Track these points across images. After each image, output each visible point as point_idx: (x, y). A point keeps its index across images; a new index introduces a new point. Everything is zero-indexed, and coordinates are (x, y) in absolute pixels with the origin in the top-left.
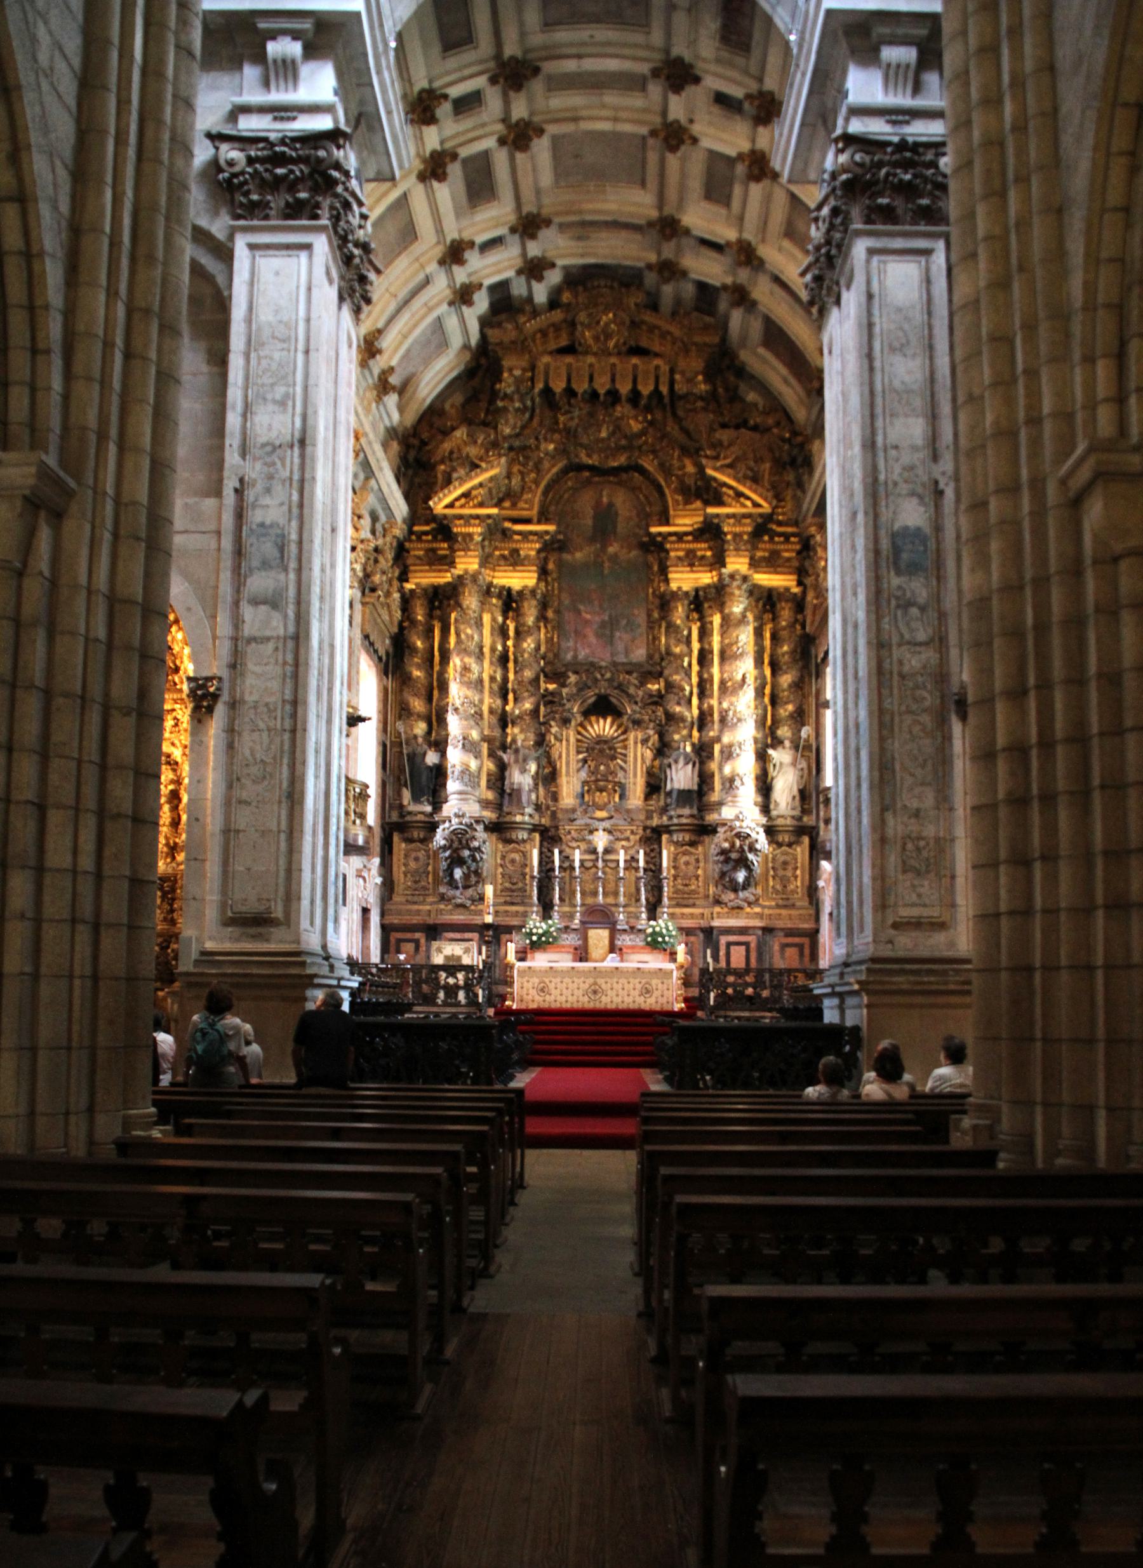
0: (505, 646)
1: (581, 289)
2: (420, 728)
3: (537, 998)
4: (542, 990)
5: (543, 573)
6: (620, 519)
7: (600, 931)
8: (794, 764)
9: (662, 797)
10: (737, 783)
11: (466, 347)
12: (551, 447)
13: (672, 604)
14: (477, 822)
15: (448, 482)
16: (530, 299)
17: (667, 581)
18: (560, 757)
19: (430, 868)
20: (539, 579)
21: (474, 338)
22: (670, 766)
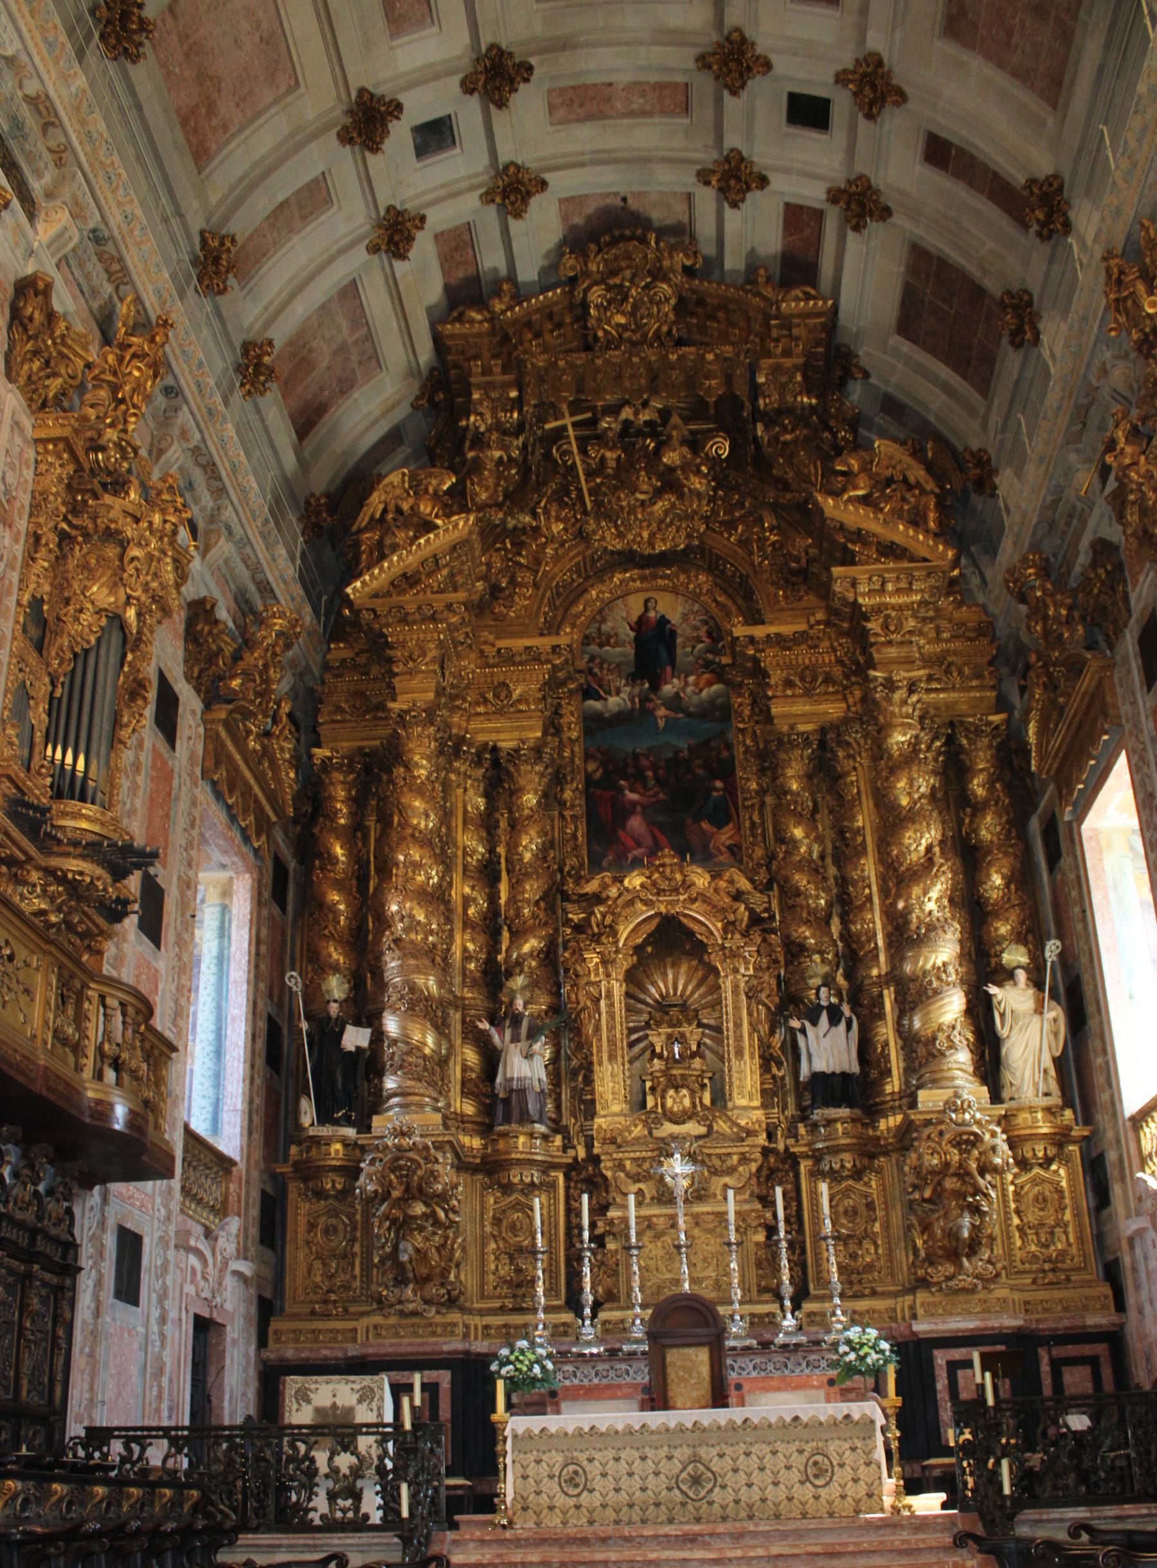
0: (491, 851)
1: (593, 247)
2: (336, 987)
3: (560, 1500)
4: (571, 1481)
5: (553, 726)
6: (679, 640)
7: (690, 1351)
8: (1039, 1010)
9: (791, 1101)
10: (941, 1042)
11: (412, 372)
12: (557, 528)
13: (783, 756)
14: (438, 1146)
15: (381, 553)
16: (512, 277)
17: (769, 719)
18: (597, 1029)
19: (357, 1248)
20: (545, 733)
21: (426, 354)
22: (803, 1031)
